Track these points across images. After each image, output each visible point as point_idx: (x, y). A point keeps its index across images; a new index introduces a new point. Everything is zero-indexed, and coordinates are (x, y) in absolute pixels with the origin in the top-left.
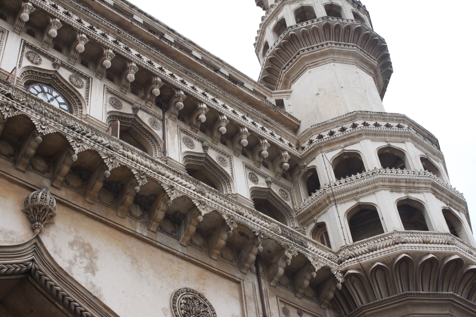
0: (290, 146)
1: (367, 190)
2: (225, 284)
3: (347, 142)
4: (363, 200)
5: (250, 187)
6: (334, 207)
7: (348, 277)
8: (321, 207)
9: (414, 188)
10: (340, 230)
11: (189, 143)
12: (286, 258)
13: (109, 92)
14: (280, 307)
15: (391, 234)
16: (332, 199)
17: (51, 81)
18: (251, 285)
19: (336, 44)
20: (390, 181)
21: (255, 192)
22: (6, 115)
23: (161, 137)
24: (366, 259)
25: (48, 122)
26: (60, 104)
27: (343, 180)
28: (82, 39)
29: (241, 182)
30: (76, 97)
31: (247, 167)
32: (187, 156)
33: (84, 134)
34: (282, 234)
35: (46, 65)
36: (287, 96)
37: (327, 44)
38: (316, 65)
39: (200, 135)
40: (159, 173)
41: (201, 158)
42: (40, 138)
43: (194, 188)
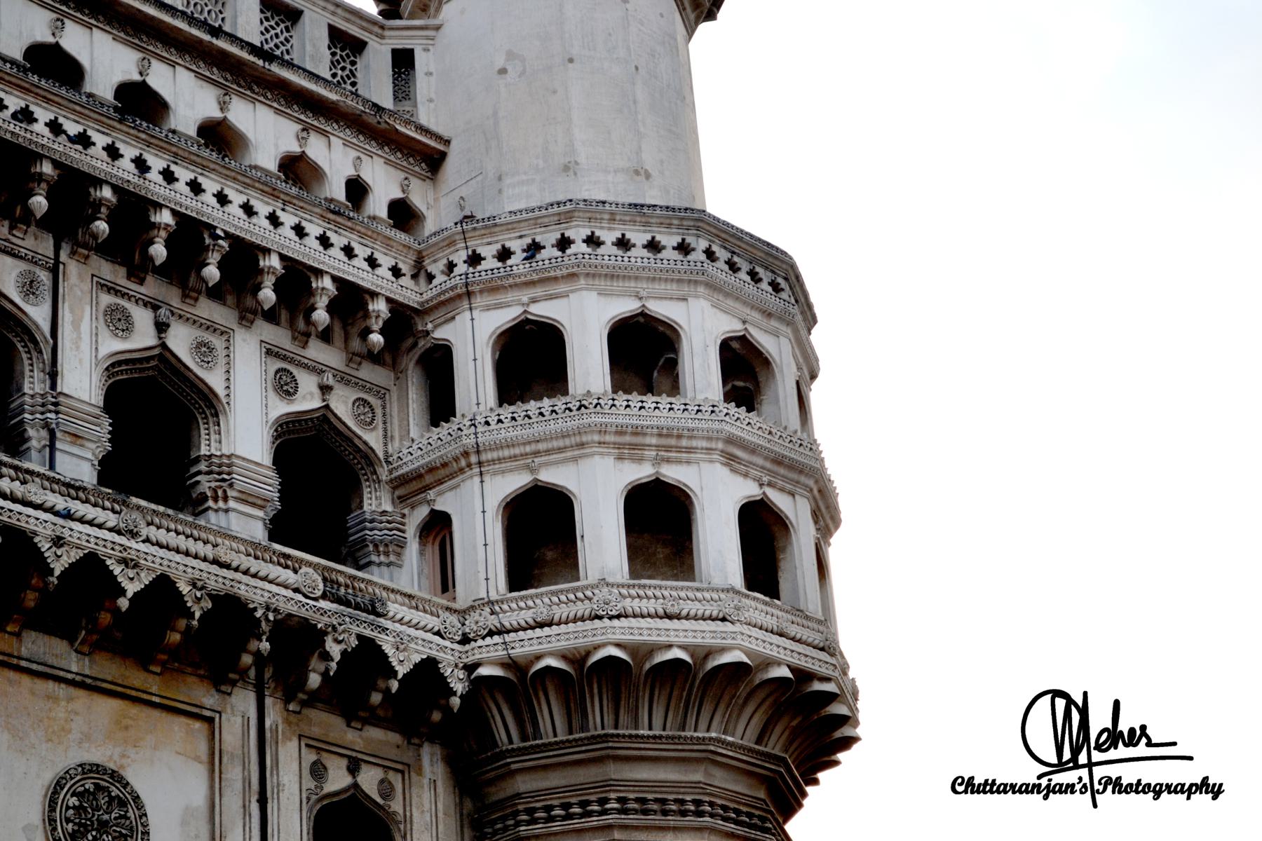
1: (560, 450)
3: (538, 291)
6: (477, 479)
11: (119, 321)
12: (326, 657)
14: (304, 764)
16: (474, 459)
18: (239, 720)
23: (46, 327)
24: (523, 646)
31: (271, 352)
32: (113, 365)
34: (324, 596)
36: (428, 38)
39: (152, 287)
43: (112, 520)
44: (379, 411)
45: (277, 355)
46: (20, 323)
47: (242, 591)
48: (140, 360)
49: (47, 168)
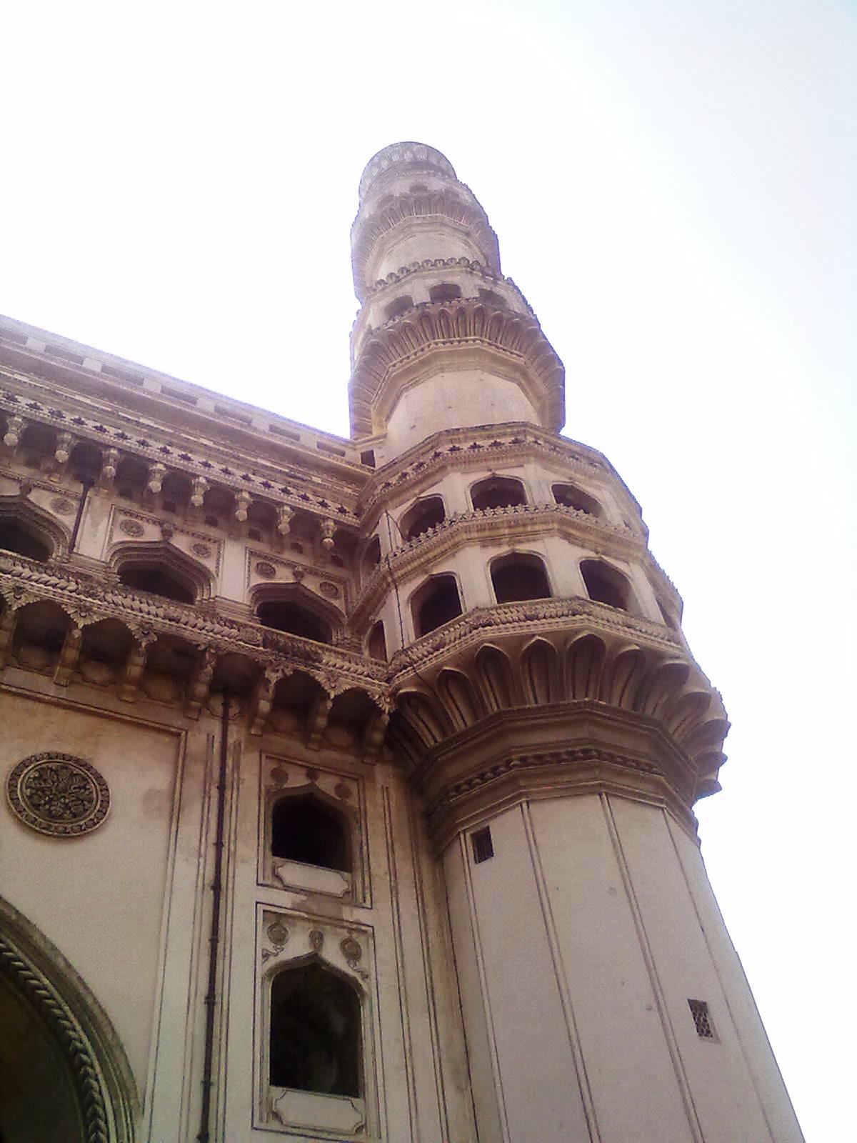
0: (342, 511)
1: (443, 553)
2: (148, 739)
3: (424, 485)
5: (253, 583)
7: (402, 701)
8: (376, 599)
9: (527, 534)
12: (268, 681)
15: (469, 615)
16: (390, 579)
18: (205, 737)
20: (481, 529)
29: (233, 576)
39: (160, 514)
43: (73, 586)
45: (259, 556)
46: (52, 524)
47: (188, 633)
48: (147, 549)
49: (67, 437)
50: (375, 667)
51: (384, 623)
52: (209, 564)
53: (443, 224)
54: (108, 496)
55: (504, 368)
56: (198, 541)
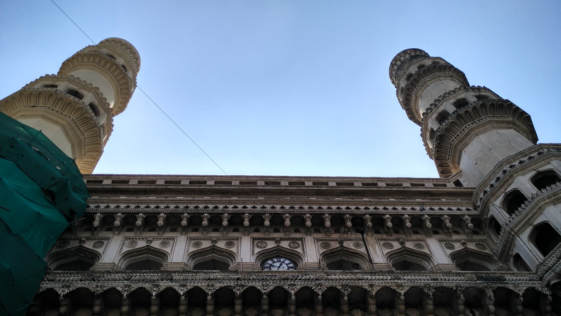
0: (468, 210)
1: (534, 214)
3: (505, 186)
4: (536, 223)
5: (448, 254)
6: (518, 238)
8: (510, 243)
10: (530, 253)
13: (318, 240)
16: (513, 233)
17: (278, 253)
19: (472, 124)
20: (549, 197)
21: (454, 257)
22: (238, 292)
23: (366, 252)
25: (268, 283)
26: (287, 265)
27: (514, 216)
28: (286, 217)
29: (439, 253)
30: (297, 255)
33: (296, 279)
35: (271, 245)
37: (466, 127)
38: (466, 145)
39: (395, 236)
40: (359, 279)
41: (402, 251)
42: (265, 296)
43: (389, 278)
44: (486, 245)
49: (348, 216)
50: (531, 275)
51: (521, 254)
52: (426, 251)
53: (439, 77)
54: (372, 235)
55: (504, 125)
56: (416, 242)
